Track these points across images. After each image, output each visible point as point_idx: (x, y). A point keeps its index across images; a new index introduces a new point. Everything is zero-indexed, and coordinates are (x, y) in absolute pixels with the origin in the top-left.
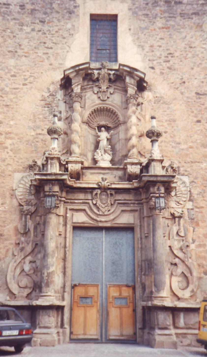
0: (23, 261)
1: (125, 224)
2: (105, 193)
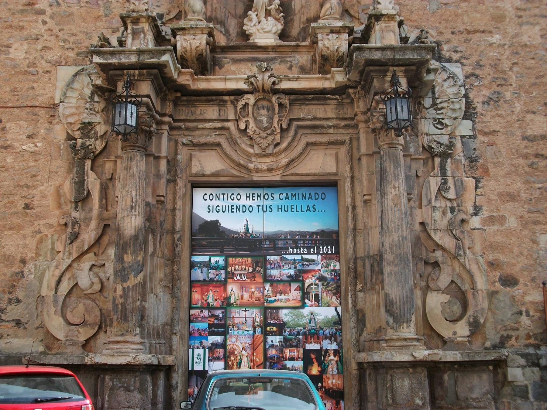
0: (75, 265)
1: (314, 174)
2: (265, 103)
